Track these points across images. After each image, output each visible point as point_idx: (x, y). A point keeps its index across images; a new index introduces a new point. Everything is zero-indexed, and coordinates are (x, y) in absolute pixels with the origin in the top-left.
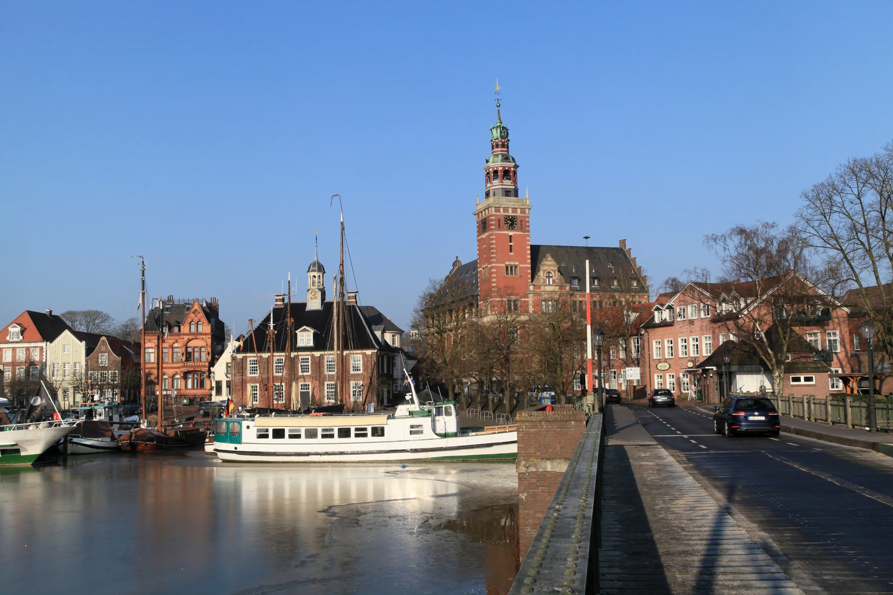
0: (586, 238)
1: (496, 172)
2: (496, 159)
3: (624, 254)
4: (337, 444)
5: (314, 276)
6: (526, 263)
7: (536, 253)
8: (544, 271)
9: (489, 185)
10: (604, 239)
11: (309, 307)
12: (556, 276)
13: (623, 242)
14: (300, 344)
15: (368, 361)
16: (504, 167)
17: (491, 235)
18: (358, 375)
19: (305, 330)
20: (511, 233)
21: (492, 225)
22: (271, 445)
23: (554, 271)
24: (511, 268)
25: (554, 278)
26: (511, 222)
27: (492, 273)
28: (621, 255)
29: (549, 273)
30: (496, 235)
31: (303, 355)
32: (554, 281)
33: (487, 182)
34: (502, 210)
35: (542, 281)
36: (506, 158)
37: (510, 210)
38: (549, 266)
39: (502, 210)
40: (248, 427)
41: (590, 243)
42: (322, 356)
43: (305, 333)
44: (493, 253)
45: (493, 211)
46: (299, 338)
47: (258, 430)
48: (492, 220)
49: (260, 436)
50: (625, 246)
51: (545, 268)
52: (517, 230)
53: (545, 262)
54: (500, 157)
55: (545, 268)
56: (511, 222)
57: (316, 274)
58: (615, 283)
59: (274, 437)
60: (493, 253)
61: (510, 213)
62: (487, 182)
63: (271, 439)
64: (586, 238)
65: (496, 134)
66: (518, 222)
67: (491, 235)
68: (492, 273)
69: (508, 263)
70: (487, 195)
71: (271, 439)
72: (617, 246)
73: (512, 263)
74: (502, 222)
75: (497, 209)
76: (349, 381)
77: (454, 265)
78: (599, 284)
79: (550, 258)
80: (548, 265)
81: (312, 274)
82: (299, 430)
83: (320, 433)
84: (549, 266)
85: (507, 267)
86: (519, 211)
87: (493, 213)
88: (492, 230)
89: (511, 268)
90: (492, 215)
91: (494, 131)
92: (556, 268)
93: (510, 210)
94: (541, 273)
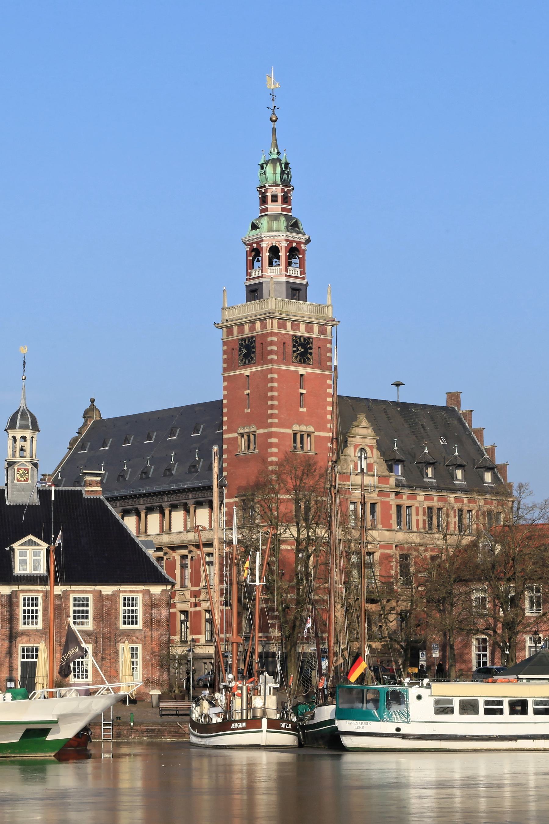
0: (398, 385)
1: (274, 251)
2: (275, 225)
3: (460, 420)
4: (506, 723)
5: (24, 438)
6: (324, 429)
7: (349, 409)
8: (356, 446)
9: (255, 273)
10: (425, 391)
11: (10, 499)
12: (374, 456)
13: (454, 397)
14: (18, 570)
15: (153, 607)
16: (291, 242)
17: (271, 371)
18: (134, 631)
19: (30, 543)
20: (303, 370)
21: (271, 352)
22: (457, 724)
23: (371, 447)
24: (302, 436)
25: (371, 461)
26: (303, 350)
27: (271, 445)
28: (455, 422)
29: (362, 450)
30: (279, 372)
31: (25, 591)
32: (370, 467)
33: (250, 265)
34: (289, 324)
35: (352, 465)
36: (294, 226)
37: (302, 326)
38: (365, 437)
39: (289, 324)
40: (419, 697)
41: (404, 396)
42: (66, 594)
43: (30, 550)
44: (272, 407)
45: (273, 326)
46: (17, 558)
47: (437, 702)
48: (272, 343)
49: (438, 712)
50: (459, 404)
51: (358, 440)
52: (312, 366)
53: (357, 430)
54: (283, 222)
55: (358, 440)
56: (303, 350)
57: (27, 433)
58: (459, 474)
59: (261, 728)
60: (272, 407)
61: (302, 332)
62: (250, 265)
63: (456, 715)
64: (398, 385)
65: (273, 174)
66: (315, 351)
67: (271, 371)
68: (271, 445)
69: (296, 427)
70: (254, 292)
71: (456, 715)
72: (443, 403)
73: (304, 428)
74: (290, 348)
75: (282, 325)
76: (116, 643)
77: (87, 415)
78: (435, 476)
79: (365, 423)
80: (363, 433)
81: (19, 433)
82: (451, 702)
83: (481, 707)
84: (365, 437)
85: (295, 435)
86: (316, 328)
87: (276, 330)
88: (271, 361)
89: (302, 436)
90: (272, 334)
91: (269, 169)
92: (373, 442)
93: (302, 326)
94: (350, 450)
